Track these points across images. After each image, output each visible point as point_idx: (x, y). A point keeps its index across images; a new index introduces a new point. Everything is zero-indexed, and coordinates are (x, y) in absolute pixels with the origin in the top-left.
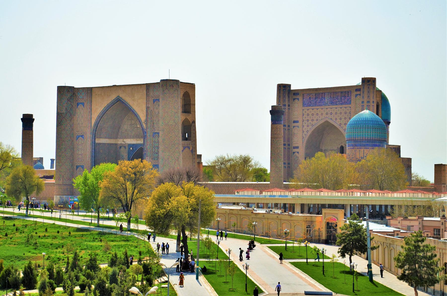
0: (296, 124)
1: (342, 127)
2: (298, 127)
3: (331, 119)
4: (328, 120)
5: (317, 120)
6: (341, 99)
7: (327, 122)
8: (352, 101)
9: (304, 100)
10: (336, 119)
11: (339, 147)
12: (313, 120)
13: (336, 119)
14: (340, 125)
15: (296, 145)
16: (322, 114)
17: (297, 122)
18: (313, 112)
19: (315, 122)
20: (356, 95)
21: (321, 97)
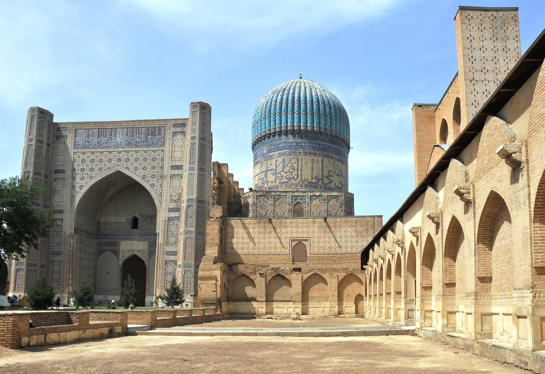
0: (60, 175)
1: (148, 182)
2: (64, 179)
3: (127, 168)
4: (119, 169)
5: (100, 169)
6: (146, 137)
7: (119, 174)
8: (167, 143)
9: (77, 138)
10: (136, 169)
11: (130, 218)
12: (92, 170)
13: (136, 169)
14: (143, 179)
15: (58, 208)
16: (110, 160)
17: (63, 171)
18: (92, 157)
19: (96, 171)
20: (175, 134)
21: (108, 134)
